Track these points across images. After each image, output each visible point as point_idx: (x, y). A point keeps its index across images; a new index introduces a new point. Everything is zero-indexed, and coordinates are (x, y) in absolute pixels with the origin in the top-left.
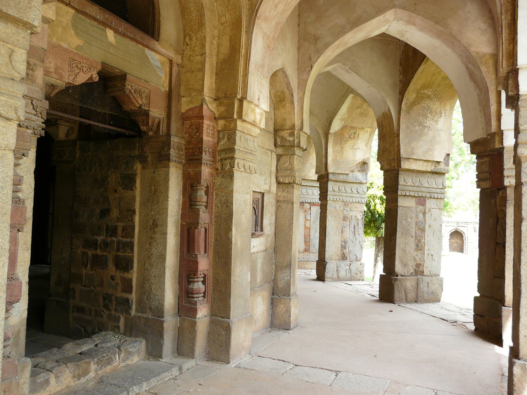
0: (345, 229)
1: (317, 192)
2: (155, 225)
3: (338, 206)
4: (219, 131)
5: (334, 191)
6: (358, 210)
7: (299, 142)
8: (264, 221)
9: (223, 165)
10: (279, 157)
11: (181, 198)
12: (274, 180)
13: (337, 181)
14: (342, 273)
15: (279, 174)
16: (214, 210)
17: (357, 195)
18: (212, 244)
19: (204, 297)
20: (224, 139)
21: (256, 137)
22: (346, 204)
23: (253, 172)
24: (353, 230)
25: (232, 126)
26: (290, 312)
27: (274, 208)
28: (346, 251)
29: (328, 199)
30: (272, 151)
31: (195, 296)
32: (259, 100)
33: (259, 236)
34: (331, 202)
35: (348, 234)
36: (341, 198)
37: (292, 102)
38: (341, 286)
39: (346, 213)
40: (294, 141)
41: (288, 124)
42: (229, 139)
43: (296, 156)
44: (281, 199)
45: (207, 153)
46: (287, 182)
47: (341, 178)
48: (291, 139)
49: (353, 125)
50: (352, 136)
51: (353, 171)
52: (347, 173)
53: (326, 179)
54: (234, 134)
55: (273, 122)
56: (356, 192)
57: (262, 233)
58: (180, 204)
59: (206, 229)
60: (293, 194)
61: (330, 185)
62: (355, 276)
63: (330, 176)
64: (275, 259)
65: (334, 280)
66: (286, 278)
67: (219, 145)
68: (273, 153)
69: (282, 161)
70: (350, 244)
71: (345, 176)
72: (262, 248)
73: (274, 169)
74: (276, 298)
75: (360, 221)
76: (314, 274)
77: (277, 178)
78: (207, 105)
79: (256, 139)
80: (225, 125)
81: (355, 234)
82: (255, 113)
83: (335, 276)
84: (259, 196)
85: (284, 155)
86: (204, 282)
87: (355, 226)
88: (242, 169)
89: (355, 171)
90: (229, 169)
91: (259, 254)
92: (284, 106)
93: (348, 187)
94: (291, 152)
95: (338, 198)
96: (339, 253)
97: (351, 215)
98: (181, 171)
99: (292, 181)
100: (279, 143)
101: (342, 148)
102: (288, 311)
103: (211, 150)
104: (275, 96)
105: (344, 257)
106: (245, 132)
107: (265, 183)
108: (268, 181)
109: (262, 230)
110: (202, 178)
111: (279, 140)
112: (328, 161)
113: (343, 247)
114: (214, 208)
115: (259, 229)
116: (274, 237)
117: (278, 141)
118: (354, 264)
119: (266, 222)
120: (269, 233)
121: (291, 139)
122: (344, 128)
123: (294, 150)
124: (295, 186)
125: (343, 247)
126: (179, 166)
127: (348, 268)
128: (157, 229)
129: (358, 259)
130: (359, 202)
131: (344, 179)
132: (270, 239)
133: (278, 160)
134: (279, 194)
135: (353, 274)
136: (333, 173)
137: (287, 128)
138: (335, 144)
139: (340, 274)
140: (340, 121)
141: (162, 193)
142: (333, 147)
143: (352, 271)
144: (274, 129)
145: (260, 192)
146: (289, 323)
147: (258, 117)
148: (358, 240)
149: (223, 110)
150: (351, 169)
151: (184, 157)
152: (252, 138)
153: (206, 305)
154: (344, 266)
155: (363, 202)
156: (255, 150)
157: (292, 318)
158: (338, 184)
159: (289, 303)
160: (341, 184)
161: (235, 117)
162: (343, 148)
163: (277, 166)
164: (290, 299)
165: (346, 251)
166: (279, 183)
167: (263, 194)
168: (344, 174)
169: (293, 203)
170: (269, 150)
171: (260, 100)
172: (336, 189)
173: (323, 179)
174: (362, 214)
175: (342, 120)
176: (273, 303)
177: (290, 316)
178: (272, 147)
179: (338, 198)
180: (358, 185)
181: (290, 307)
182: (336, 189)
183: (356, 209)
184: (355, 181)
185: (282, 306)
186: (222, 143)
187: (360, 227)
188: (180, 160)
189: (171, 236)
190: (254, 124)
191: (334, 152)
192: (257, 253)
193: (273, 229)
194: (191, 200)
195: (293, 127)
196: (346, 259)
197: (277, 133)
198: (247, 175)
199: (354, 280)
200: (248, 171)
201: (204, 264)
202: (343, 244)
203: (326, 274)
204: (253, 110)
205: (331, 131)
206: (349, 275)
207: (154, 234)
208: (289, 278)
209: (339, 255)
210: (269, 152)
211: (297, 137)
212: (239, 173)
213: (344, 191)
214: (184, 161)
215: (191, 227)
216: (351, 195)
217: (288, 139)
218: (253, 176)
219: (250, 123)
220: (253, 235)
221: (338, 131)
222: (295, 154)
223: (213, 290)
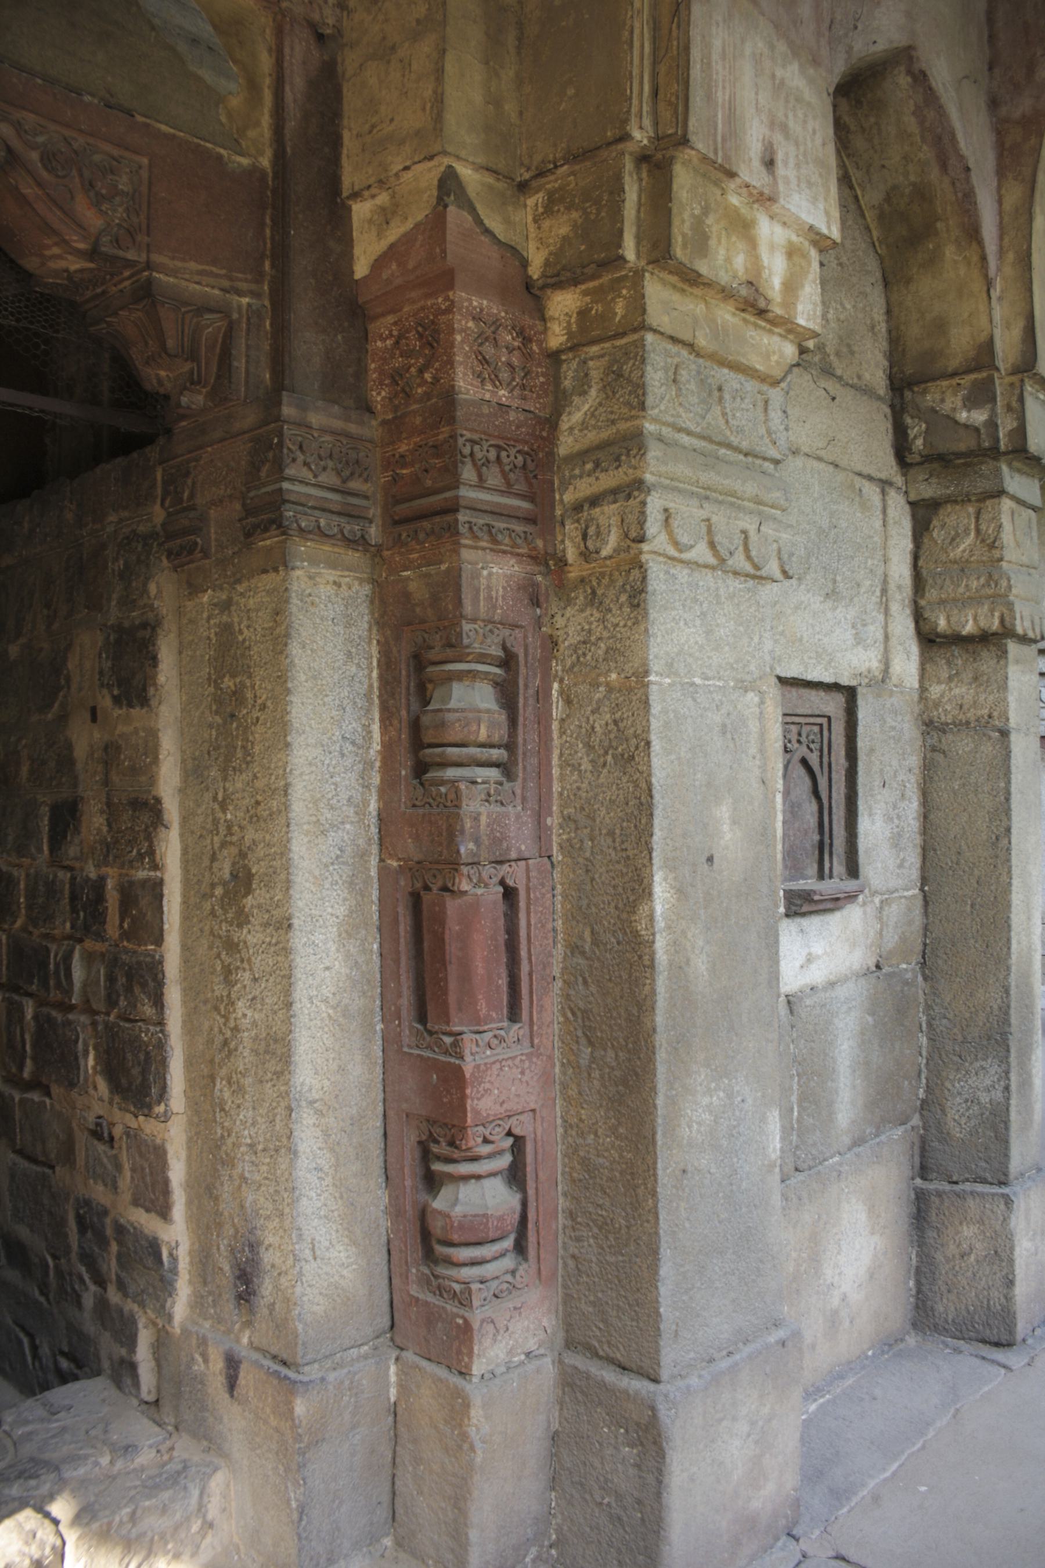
2: (242, 881)
4: (555, 357)
7: (1020, 432)
8: (864, 824)
9: (585, 536)
10: (923, 515)
11: (376, 728)
12: (903, 625)
15: (932, 594)
16: (556, 788)
18: (556, 971)
19: (520, 1248)
20: (583, 393)
21: (776, 383)
23: (773, 568)
25: (620, 308)
26: (1011, 1262)
27: (914, 761)
30: (885, 484)
31: (464, 1254)
32: (770, 163)
33: (836, 903)
37: (973, 233)
40: (992, 424)
41: (960, 342)
42: (609, 389)
43: (1007, 504)
44: (947, 713)
45: (493, 478)
46: (969, 628)
48: (979, 417)
54: (638, 355)
55: (885, 345)
57: (851, 885)
58: (368, 765)
59: (509, 894)
60: (1003, 687)
64: (928, 1007)
66: (984, 1098)
67: (565, 424)
68: (892, 493)
69: (938, 534)
72: (858, 958)
73: (901, 571)
74: (939, 1194)
77: (918, 616)
78: (472, 210)
79: (775, 395)
80: (583, 313)
82: (752, 243)
84: (833, 705)
85: (951, 500)
86: (516, 1176)
88: (700, 552)
90: (617, 551)
91: (841, 992)
92: (933, 261)
94: (983, 485)
98: (367, 589)
99: (995, 625)
100: (919, 442)
102: (1001, 1255)
103: (512, 457)
104: (881, 217)
106: (702, 342)
107: (859, 640)
108: (874, 630)
109: (853, 870)
110: (468, 608)
111: (916, 429)
114: (555, 772)
115: (839, 868)
116: (919, 902)
117: (912, 433)
119: (874, 828)
120: (892, 884)
121: (979, 417)
123: (998, 471)
124: (1013, 647)
126: (353, 556)
128: (249, 901)
132: (894, 912)
133: (920, 530)
134: (936, 690)
137: (954, 364)
141: (263, 707)
144: (891, 378)
145: (835, 687)
146: (1007, 1316)
147: (775, 271)
149: (564, 230)
151: (375, 511)
152: (751, 386)
153: (534, 1295)
156: (773, 453)
157: (1020, 1290)
159: (1005, 1220)
161: (629, 251)
163: (916, 557)
164: (1008, 1201)
166: (930, 640)
167: (850, 693)
169: (1004, 733)
170: (870, 478)
171: (781, 170)
176: (922, 1216)
177: (1010, 1283)
178: (886, 465)
181: (1010, 1238)
185: (968, 1231)
186: (573, 417)
188: (352, 528)
189: (318, 938)
190: (754, 306)
192: (832, 984)
193: (913, 858)
194: (417, 743)
195: (984, 355)
197: (908, 394)
198: (735, 584)
200: (739, 561)
201: (509, 1078)
204: (744, 228)
207: (240, 926)
208: (998, 1095)
210: (872, 492)
211: (1009, 408)
212: (683, 574)
214: (374, 533)
215: (427, 888)
217: (963, 416)
218: (768, 592)
219: (726, 294)
220: (801, 905)
222: (1001, 493)
223: (571, 1215)
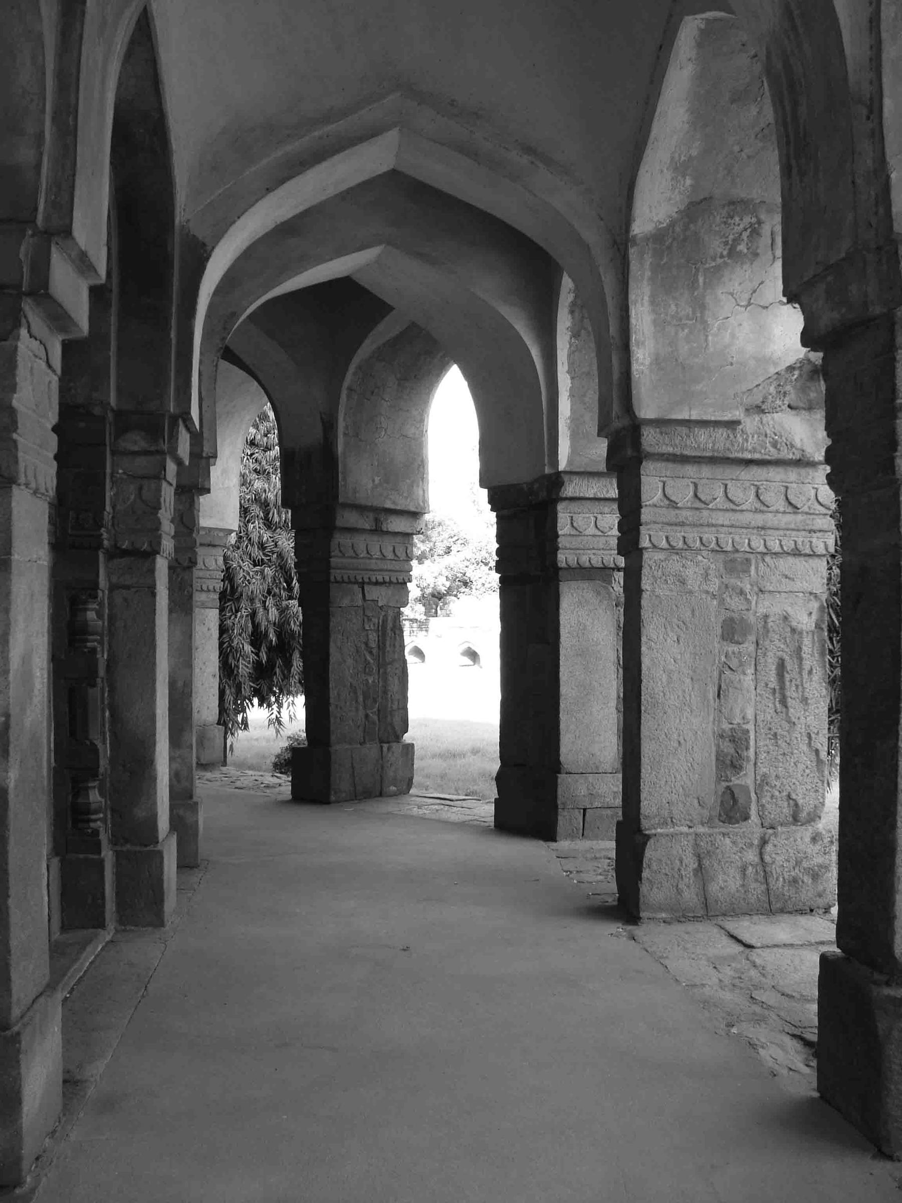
0: (735, 677)
1: (611, 520)
3: (692, 573)
5: (673, 505)
6: (798, 585)
13: (684, 459)
14: (727, 882)
17: (789, 518)
22: (736, 563)
24: (774, 683)
28: (747, 779)
29: (645, 543)
34: (660, 556)
35: (750, 704)
36: (709, 536)
38: (710, 941)
39: (735, 603)
47: (705, 441)
49: (740, 193)
50: (742, 247)
51: (759, 409)
52: (728, 416)
53: (629, 452)
56: (781, 505)
61: (653, 483)
62: (788, 891)
63: (650, 439)
65: (681, 915)
70: (758, 745)
71: (721, 434)
75: (807, 642)
76: (602, 881)
81: (784, 702)
83: (690, 896)
87: (781, 666)
89: (775, 410)
93: (741, 485)
95: (692, 536)
96: (710, 791)
97: (761, 610)
101: (700, 306)
105: (732, 809)
112: (635, 367)
113: (730, 761)
118: (781, 841)
122: (696, 209)
125: (730, 761)
127: (751, 856)
129: (803, 815)
130: (796, 553)
131: (720, 446)
135: (777, 885)
136: (661, 423)
138: (665, 285)
139: (713, 888)
140: (668, 175)
142: (653, 302)
143: (775, 870)
148: (800, 728)
150: (748, 400)
154: (734, 847)
155: (821, 550)
158: (690, 470)
160: (706, 471)
162: (703, 307)
165: (747, 779)
168: (717, 424)
172: (683, 494)
173: (626, 454)
174: (815, 605)
175: (680, 168)
179: (692, 536)
180: (792, 474)
182: (683, 494)
183: (786, 585)
184: (773, 454)
187: (807, 664)
191: (660, 325)
196: (746, 818)
199: (782, 911)
202: (728, 748)
203: (644, 888)
205: (640, 227)
206: (756, 889)
209: (711, 800)
213: (720, 501)
216: (759, 519)
221: (672, 224)
